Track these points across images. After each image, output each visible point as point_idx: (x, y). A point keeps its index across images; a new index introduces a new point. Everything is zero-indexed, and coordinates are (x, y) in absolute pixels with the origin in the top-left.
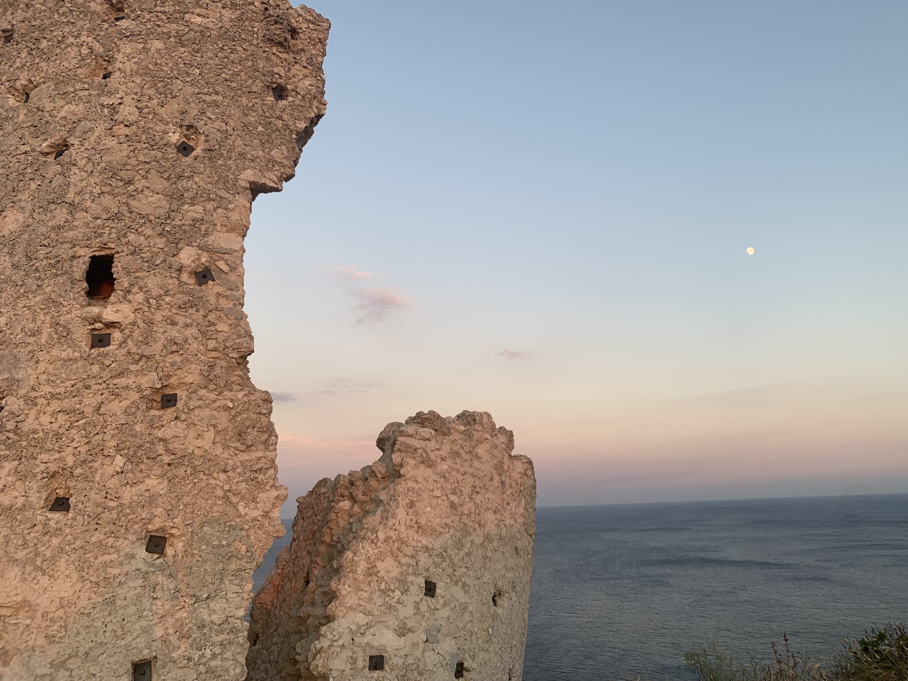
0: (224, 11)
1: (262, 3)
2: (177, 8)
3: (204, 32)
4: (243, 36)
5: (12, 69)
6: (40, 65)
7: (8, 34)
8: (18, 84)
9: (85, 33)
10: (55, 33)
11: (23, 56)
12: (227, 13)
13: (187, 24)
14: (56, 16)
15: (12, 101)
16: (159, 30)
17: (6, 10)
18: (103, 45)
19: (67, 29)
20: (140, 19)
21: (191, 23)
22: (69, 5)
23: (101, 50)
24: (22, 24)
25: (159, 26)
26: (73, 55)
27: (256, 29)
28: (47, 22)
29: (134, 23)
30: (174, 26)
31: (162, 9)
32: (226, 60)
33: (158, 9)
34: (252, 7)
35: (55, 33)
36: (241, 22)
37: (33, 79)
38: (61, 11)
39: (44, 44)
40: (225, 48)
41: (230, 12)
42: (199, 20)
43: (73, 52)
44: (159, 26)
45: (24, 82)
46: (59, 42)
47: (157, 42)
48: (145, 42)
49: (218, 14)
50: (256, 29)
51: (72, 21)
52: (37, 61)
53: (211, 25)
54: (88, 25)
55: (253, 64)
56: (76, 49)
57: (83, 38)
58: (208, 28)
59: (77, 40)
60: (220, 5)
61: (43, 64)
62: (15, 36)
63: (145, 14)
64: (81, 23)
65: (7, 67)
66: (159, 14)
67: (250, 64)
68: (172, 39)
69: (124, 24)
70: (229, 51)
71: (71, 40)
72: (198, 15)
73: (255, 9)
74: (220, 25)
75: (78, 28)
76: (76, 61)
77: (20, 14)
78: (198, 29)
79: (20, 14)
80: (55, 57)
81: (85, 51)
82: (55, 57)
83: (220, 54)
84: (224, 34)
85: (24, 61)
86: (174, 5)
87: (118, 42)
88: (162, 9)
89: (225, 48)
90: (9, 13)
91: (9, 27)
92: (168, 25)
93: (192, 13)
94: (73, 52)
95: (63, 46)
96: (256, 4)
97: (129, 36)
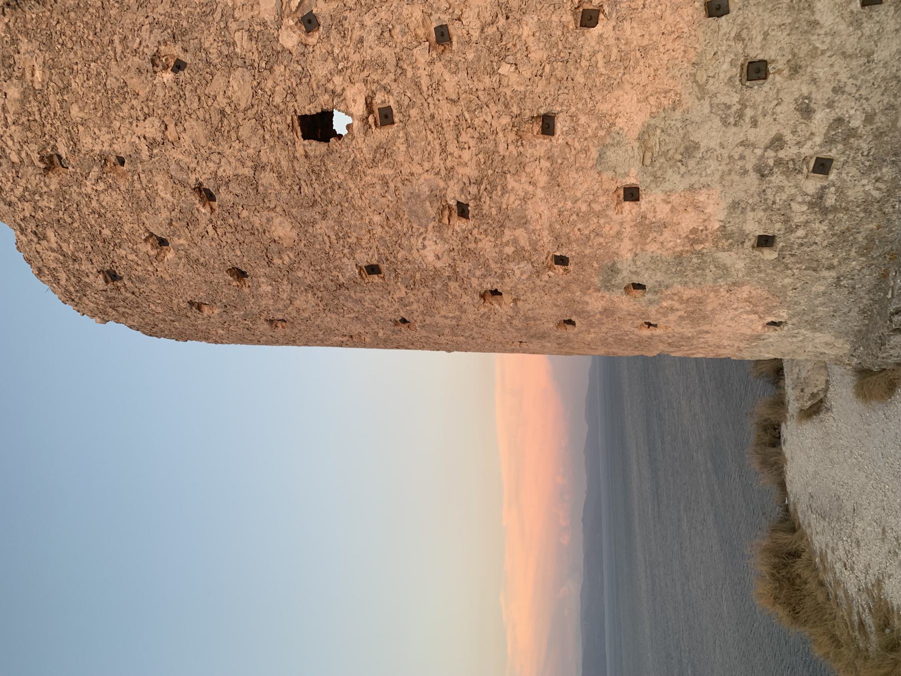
0: (22, 51)
1: (4, 14)
2: (31, 98)
3: (48, 66)
4: (44, 26)
5: (140, 262)
6: (127, 231)
7: (109, 278)
8: (153, 253)
9: (83, 189)
10: (93, 222)
11: (124, 253)
12: (24, 46)
13: (45, 84)
14: (76, 225)
15: (170, 255)
16: (59, 112)
17: (87, 285)
18: (90, 168)
19: (86, 211)
20: (53, 134)
21: (43, 81)
22: (61, 213)
23: (96, 169)
24: (94, 261)
25: (55, 113)
26: (109, 198)
27: (34, 16)
28: (84, 234)
29: (59, 140)
30: (51, 98)
31: (36, 113)
32: (74, 39)
33: (37, 117)
34: (11, 24)
35: (93, 222)
36: (30, 32)
37: (143, 238)
38: (69, 220)
39: (107, 232)
40: (61, 41)
41: (21, 44)
42: (38, 74)
43: (106, 199)
44: (55, 113)
45: (149, 247)
46: (100, 216)
47: (73, 112)
48: (76, 124)
49: (27, 55)
50: (34, 16)
51: (75, 206)
52: (125, 236)
53: (40, 60)
54: (75, 188)
55: (73, 10)
56: (102, 196)
57: (89, 191)
58: (44, 63)
59: (93, 196)
60: (16, 56)
61: (126, 228)
62: (107, 267)
63: (46, 130)
64: (74, 195)
65: (139, 268)
66: (43, 115)
67: (72, 14)
68: (66, 97)
69: (63, 151)
70: (63, 38)
71: (94, 204)
72: (33, 75)
73: (12, 20)
74: (37, 51)
75: (80, 198)
76: (114, 193)
77: (85, 266)
78: (48, 72)
79: (85, 266)
80: (116, 217)
81: (101, 186)
82: (116, 217)
83: (69, 45)
84: (48, 44)
85: (129, 251)
86: (30, 102)
87: (83, 152)
88: (36, 113)
89: (61, 41)
90: (87, 280)
91: (101, 276)
92: (52, 104)
93: (32, 82)
94: (106, 199)
95: (103, 211)
96: (6, 20)
97: (74, 142)
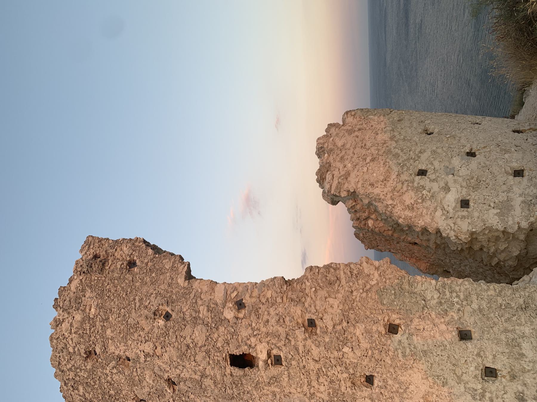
0: (87, 296)
4: (100, 285)
9: (104, 371)
10: (106, 387)
12: (88, 294)
13: (96, 316)
14: (96, 386)
16: (100, 331)
18: (111, 361)
19: (103, 381)
20: (95, 342)
23: (114, 362)
25: (98, 332)
26: (118, 377)
27: (96, 278)
28: (99, 391)
29: (97, 345)
32: (115, 295)
33: (88, 332)
34: (83, 280)
35: (106, 387)
36: (93, 286)
39: (112, 392)
40: (108, 295)
41: (87, 292)
43: (116, 377)
44: (98, 332)
46: (111, 384)
47: (107, 333)
48: (108, 339)
50: (96, 278)
52: (122, 396)
53: (96, 303)
54: (100, 369)
55: (116, 279)
56: (114, 376)
57: (108, 372)
60: (83, 298)
61: (124, 392)
64: (99, 373)
67: (116, 281)
68: (105, 324)
69: (98, 351)
70: (110, 293)
71: (109, 378)
72: (90, 310)
74: (95, 298)
76: (121, 375)
81: (115, 371)
83: (112, 298)
84: (100, 296)
86: (86, 324)
87: (109, 353)
89: (108, 295)
93: (89, 313)
94: (116, 377)
95: (113, 382)
96: (81, 278)
97: (105, 348)
